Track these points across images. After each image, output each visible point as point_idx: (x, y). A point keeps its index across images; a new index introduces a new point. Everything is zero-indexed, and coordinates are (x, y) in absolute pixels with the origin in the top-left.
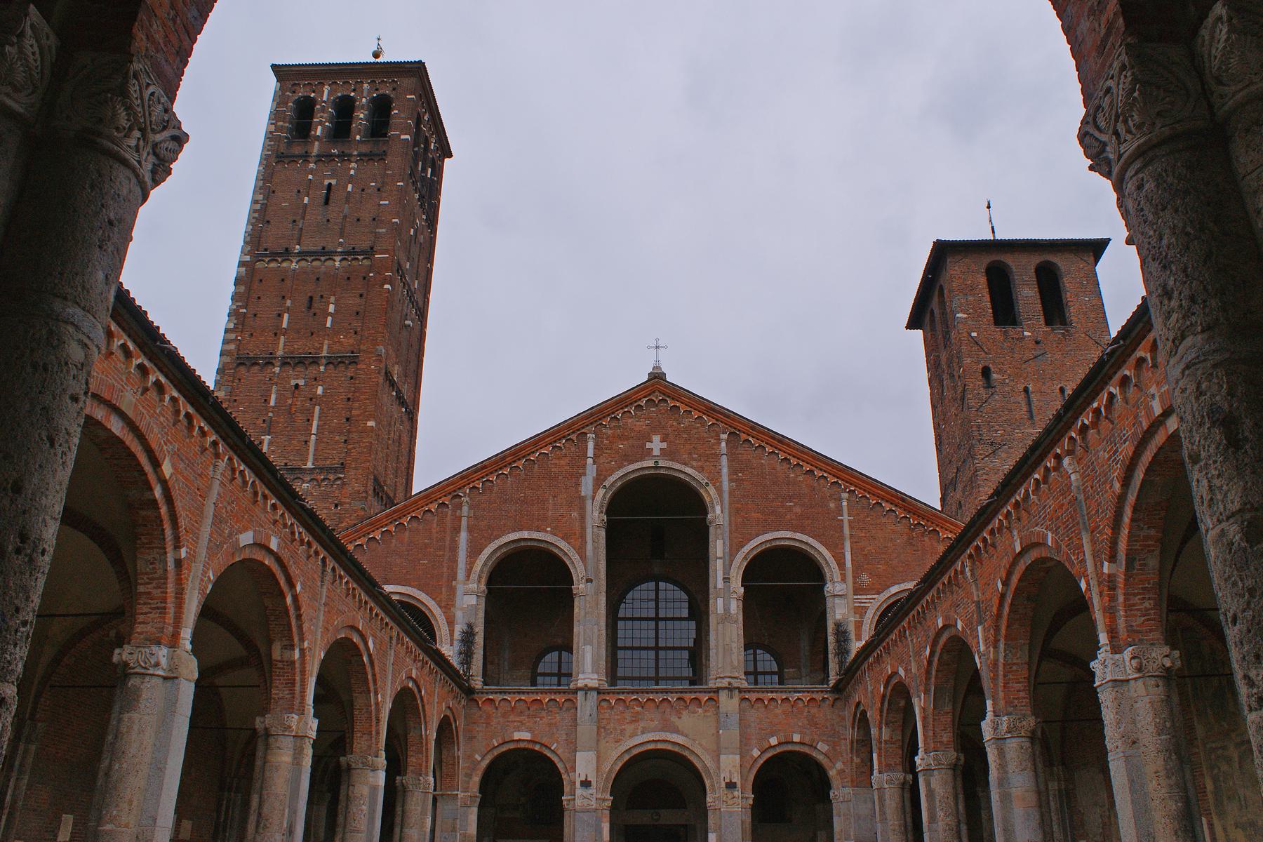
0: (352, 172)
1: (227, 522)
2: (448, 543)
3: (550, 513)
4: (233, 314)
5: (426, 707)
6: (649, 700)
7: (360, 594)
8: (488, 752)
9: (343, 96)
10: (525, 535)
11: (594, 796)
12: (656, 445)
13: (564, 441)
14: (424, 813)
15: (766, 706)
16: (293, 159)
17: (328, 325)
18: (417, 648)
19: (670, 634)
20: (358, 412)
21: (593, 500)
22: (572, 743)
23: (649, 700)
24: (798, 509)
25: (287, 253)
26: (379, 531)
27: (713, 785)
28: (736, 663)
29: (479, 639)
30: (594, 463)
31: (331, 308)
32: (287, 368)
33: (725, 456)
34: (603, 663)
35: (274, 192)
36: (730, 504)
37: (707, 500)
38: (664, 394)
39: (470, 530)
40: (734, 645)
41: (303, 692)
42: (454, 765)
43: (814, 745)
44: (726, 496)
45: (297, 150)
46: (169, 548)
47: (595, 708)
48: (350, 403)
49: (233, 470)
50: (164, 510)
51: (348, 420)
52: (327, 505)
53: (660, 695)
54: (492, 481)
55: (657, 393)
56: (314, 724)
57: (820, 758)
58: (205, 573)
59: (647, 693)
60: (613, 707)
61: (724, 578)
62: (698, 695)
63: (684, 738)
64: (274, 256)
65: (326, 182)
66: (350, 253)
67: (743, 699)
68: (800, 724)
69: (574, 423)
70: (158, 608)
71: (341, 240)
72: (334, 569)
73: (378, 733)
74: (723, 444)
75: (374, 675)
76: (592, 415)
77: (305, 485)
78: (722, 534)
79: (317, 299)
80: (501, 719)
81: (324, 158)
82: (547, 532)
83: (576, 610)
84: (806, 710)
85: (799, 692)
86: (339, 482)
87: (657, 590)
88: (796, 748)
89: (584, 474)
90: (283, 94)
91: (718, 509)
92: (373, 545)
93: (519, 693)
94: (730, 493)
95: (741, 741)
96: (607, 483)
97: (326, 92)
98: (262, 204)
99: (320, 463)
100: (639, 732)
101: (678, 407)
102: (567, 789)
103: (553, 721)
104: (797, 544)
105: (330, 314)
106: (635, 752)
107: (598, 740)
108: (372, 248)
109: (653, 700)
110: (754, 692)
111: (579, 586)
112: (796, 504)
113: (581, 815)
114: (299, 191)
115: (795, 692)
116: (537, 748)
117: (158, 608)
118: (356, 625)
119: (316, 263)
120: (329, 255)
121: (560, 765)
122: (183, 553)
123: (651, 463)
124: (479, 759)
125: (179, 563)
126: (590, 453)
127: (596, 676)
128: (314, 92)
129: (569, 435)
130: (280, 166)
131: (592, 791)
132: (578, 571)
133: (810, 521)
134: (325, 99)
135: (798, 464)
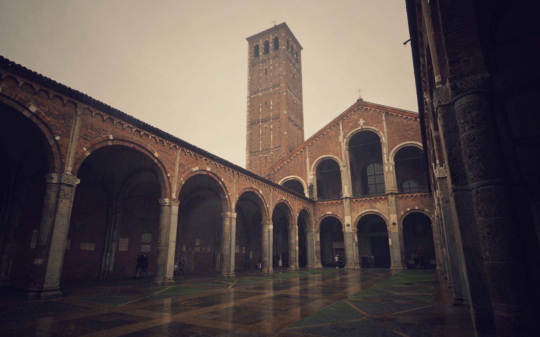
0: (271, 63)
1: (186, 166)
2: (304, 162)
3: (331, 149)
4: (248, 111)
5: (292, 207)
6: (365, 200)
7: (252, 179)
8: (321, 218)
9: (265, 41)
10: (325, 156)
11: (351, 229)
12: (361, 122)
13: (333, 127)
14: (295, 235)
15: (405, 199)
17: (271, 108)
18: (284, 192)
19: (379, 179)
20: (282, 130)
21: (343, 142)
22: (343, 214)
23: (365, 200)
24: (412, 133)
25: (258, 91)
26: (286, 162)
27: (389, 224)
28: (393, 186)
29: (315, 187)
30: (343, 131)
31: (271, 104)
32: (263, 122)
33: (384, 121)
34: (351, 190)
35: (252, 75)
36: (387, 136)
37: (380, 136)
38: (362, 105)
39: (309, 157)
40: (392, 180)
41: (231, 206)
42: (311, 222)
43: (423, 210)
44: (386, 134)
46: (164, 174)
47: (349, 204)
48: (280, 128)
49: (185, 152)
50: (159, 165)
51: (280, 133)
52: (278, 157)
53: (369, 198)
54: (314, 143)
55: (360, 106)
56: (236, 214)
57: (426, 214)
58: (179, 179)
59: (365, 198)
60: (355, 203)
61: (387, 160)
62: (381, 197)
63: (378, 210)
65: (265, 68)
66: (274, 86)
67: (397, 197)
68: (418, 203)
69: (335, 121)
70: (165, 189)
71: (271, 84)
72: (238, 173)
73: (269, 215)
74: (384, 117)
75: (264, 200)
76: (340, 117)
77: (271, 153)
78: (385, 146)
79: (267, 102)
80: (323, 209)
81: (264, 61)
82: (330, 154)
83: (342, 176)
84: (420, 198)
85: (416, 193)
86: (280, 150)
87: (374, 166)
88: (417, 211)
89: (340, 135)
90: (250, 46)
91: (383, 138)
92: (285, 165)
93: (327, 201)
94: (387, 132)
95: (397, 210)
96: (347, 137)
97: (261, 41)
98: (250, 79)
99: (274, 147)
100: (364, 208)
101: (367, 108)
102: (343, 227)
103: (337, 208)
104: (413, 145)
105: (271, 105)
106: (363, 215)
107: (351, 213)
109: (367, 200)
110: (400, 194)
111: (342, 169)
112: (411, 132)
113: (348, 234)
114: (259, 73)
115: (415, 193)
116: (334, 216)
117: (165, 189)
118: (253, 187)
119: (266, 92)
121: (341, 221)
122: (169, 175)
123: (360, 128)
124: (318, 220)
125: (168, 178)
126: (341, 128)
127: (349, 194)
128: (258, 42)
129: (334, 124)
130: (253, 67)
131: (350, 227)
132: (341, 164)
133: (417, 137)
134: (261, 44)
135: (411, 118)
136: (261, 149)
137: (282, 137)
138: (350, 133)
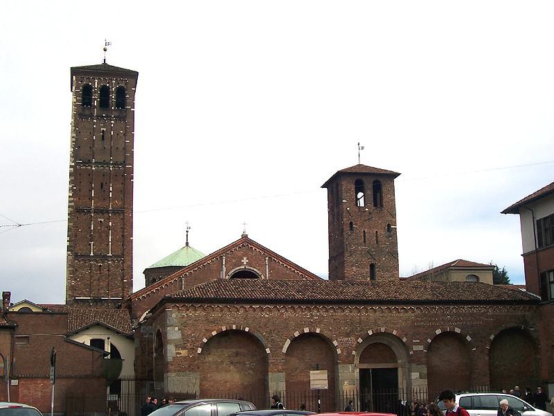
12: (245, 261)
16: (86, 117)
25: (89, 162)
31: (111, 190)
45: (87, 112)
64: (84, 163)
65: (102, 129)
66: (115, 164)
81: (99, 117)
89: (222, 270)
108: (124, 162)
120: (108, 164)
136: (92, 254)
137: (126, 243)
138: (234, 270)
